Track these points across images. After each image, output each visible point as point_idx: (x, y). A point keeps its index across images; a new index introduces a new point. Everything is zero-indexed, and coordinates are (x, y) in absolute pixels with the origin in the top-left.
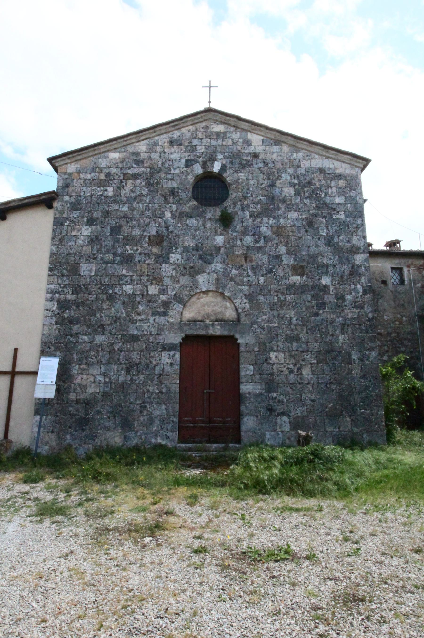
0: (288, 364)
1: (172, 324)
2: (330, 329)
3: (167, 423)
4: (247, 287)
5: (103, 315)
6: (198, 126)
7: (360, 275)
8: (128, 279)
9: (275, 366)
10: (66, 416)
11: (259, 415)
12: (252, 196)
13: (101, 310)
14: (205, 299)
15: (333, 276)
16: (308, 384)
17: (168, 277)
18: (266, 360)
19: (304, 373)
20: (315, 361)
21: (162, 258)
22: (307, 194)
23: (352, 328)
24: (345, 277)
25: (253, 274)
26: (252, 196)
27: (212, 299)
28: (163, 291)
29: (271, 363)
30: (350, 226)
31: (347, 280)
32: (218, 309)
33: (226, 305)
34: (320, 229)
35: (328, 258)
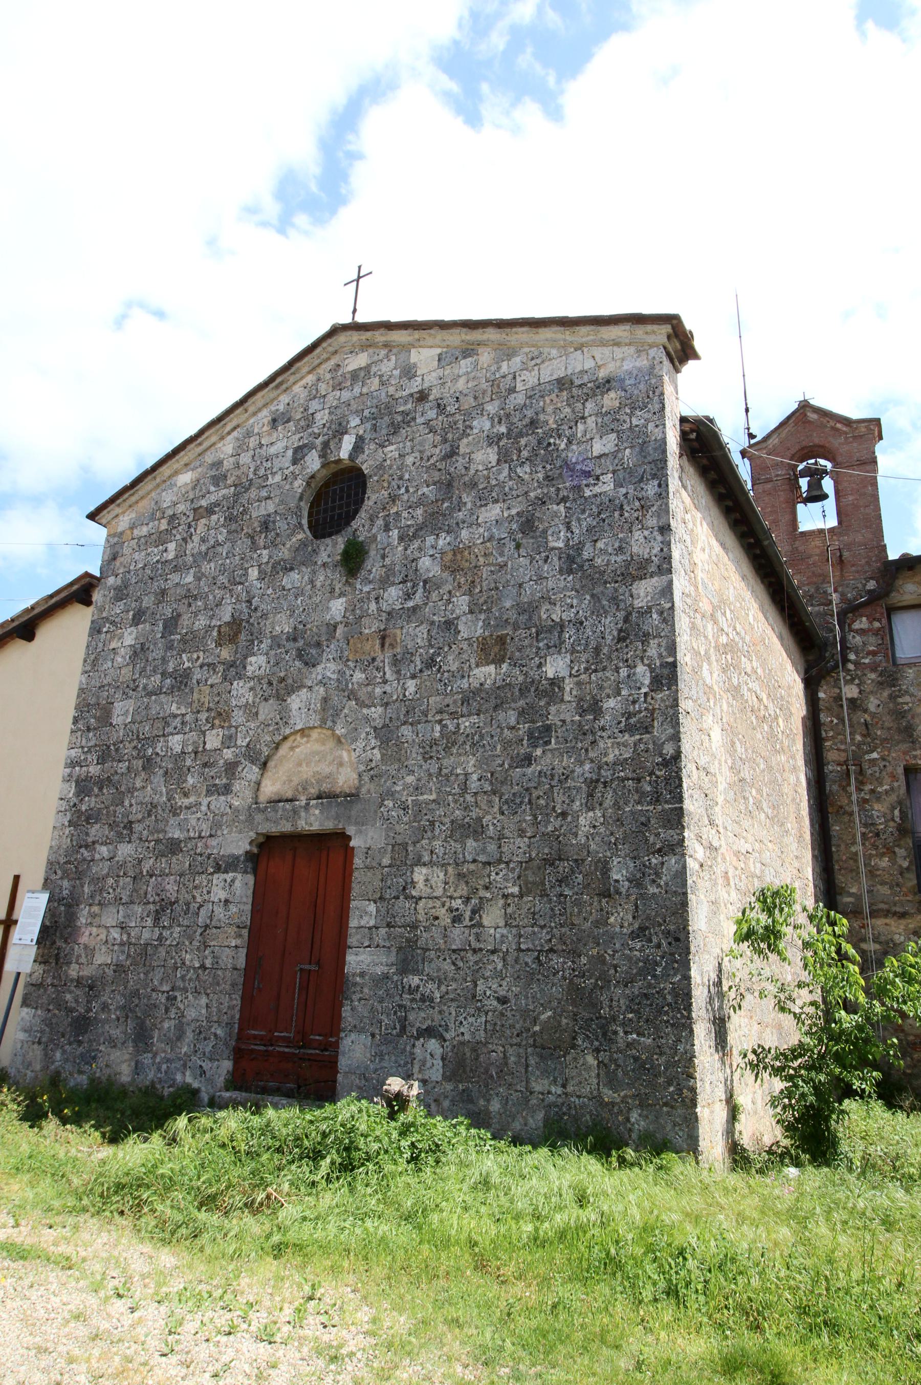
0: (451, 897)
1: (237, 811)
2: (559, 798)
3: (205, 1039)
4: (380, 710)
5: (133, 801)
6: (320, 371)
7: (646, 638)
8: (177, 722)
9: (422, 904)
10: (60, 1010)
11: (377, 1031)
12: (407, 491)
13: (131, 791)
14: (305, 747)
15: (573, 651)
16: (493, 952)
17: (240, 707)
18: (404, 889)
19: (486, 921)
20: (516, 890)
21: (234, 669)
22: (525, 454)
23: (615, 791)
24: (605, 650)
25: (395, 676)
26: (407, 491)
27: (317, 747)
28: (229, 741)
29: (413, 897)
30: (626, 508)
31: (610, 658)
32: (325, 768)
33: (341, 757)
34: (549, 532)
35: (565, 604)
